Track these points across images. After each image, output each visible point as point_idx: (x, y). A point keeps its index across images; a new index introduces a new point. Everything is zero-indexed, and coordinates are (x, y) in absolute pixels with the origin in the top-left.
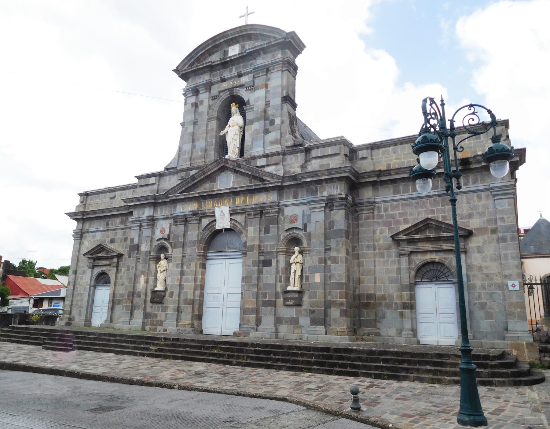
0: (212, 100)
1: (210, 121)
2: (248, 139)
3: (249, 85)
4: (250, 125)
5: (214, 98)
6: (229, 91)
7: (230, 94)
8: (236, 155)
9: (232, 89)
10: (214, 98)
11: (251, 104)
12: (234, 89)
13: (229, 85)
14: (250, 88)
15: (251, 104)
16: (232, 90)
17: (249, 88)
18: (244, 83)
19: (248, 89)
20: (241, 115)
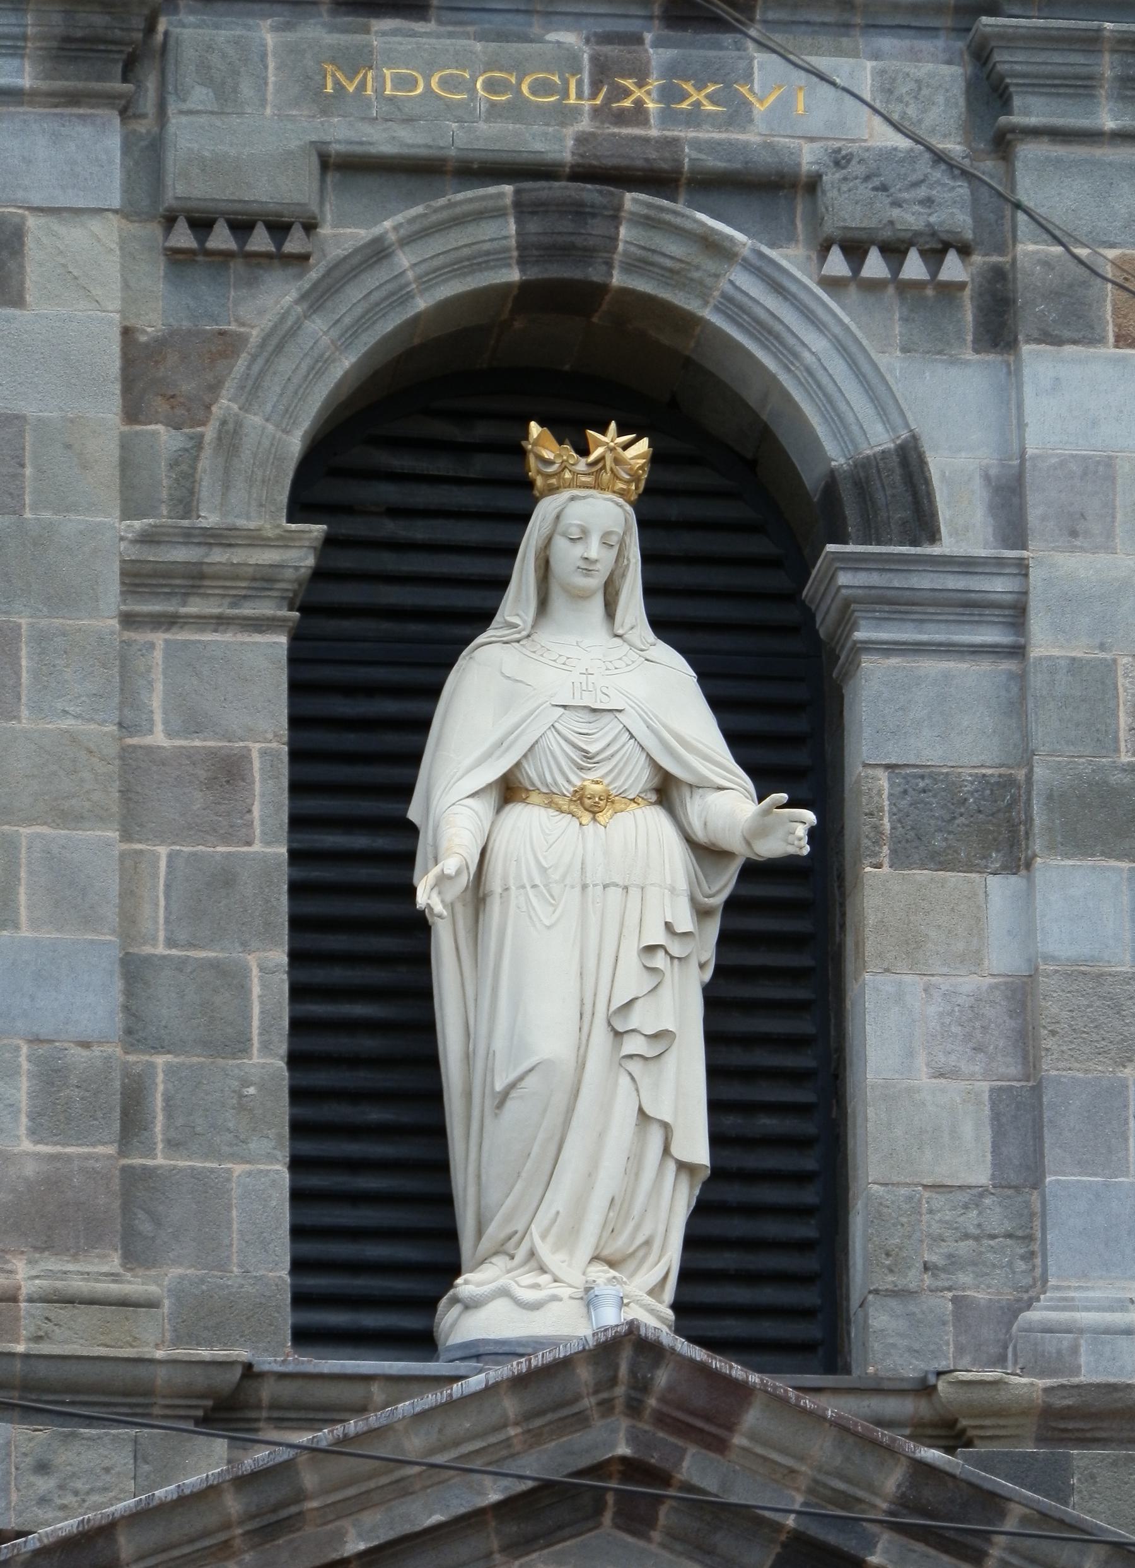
0: (177, 259)
1: (170, 621)
2: (923, 1079)
3: (911, 219)
4: (942, 861)
5: (221, 239)
6: (523, 209)
7: (526, 254)
8: (655, 1291)
9: (590, 193)
10: (221, 239)
11: (947, 546)
12: (632, 200)
13: (517, 110)
14: (914, 267)
15: (947, 546)
16: (580, 211)
17: (894, 251)
18: (808, 158)
19: (875, 266)
20: (662, 626)
